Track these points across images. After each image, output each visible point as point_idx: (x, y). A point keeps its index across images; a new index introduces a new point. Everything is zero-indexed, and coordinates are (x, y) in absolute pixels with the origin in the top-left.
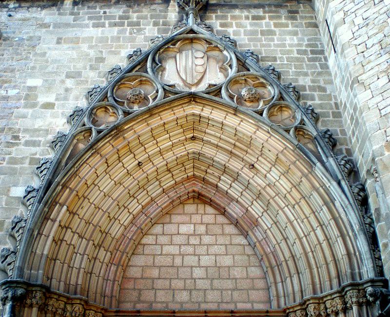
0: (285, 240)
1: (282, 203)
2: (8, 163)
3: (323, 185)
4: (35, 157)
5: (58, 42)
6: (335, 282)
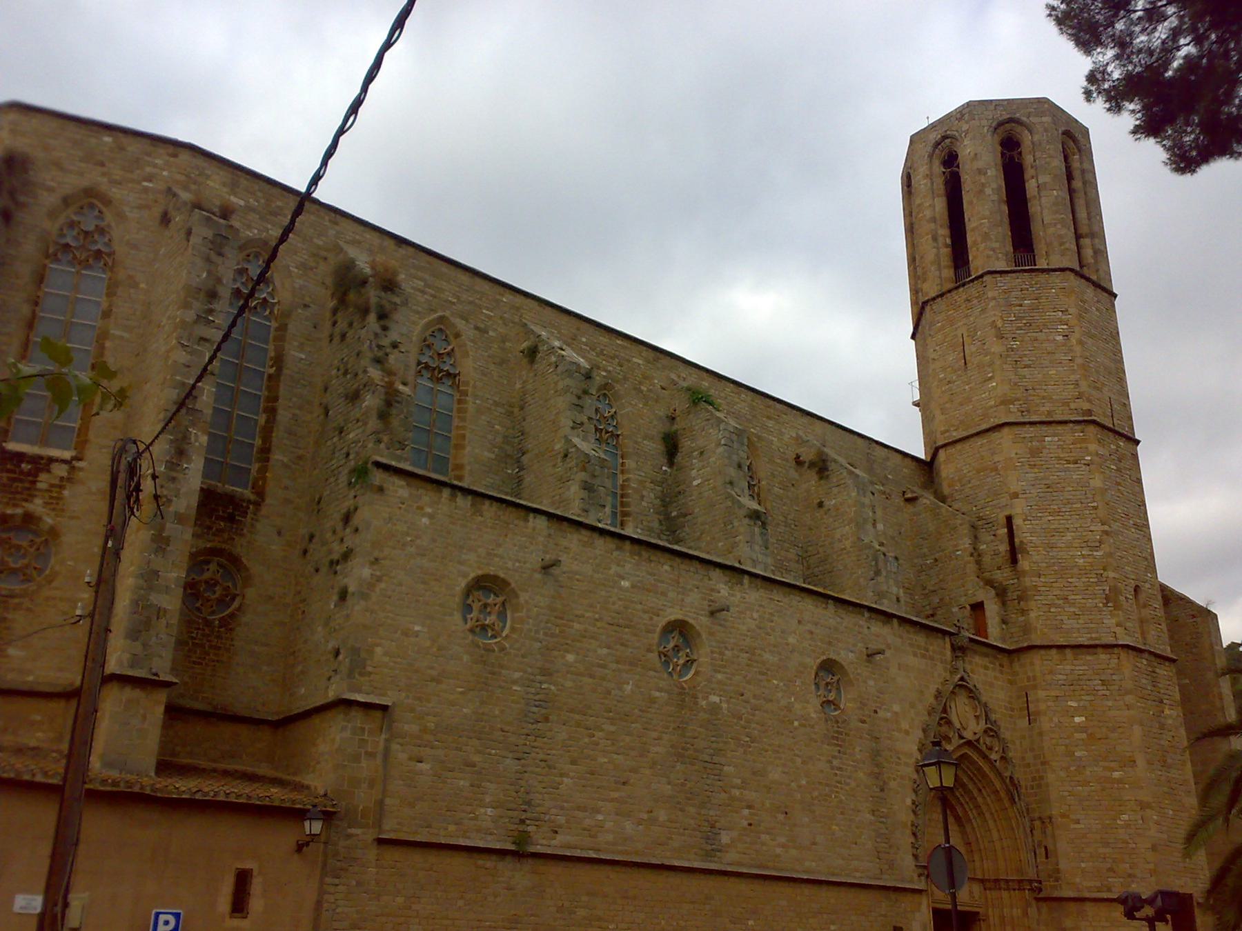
5: (899, 669)
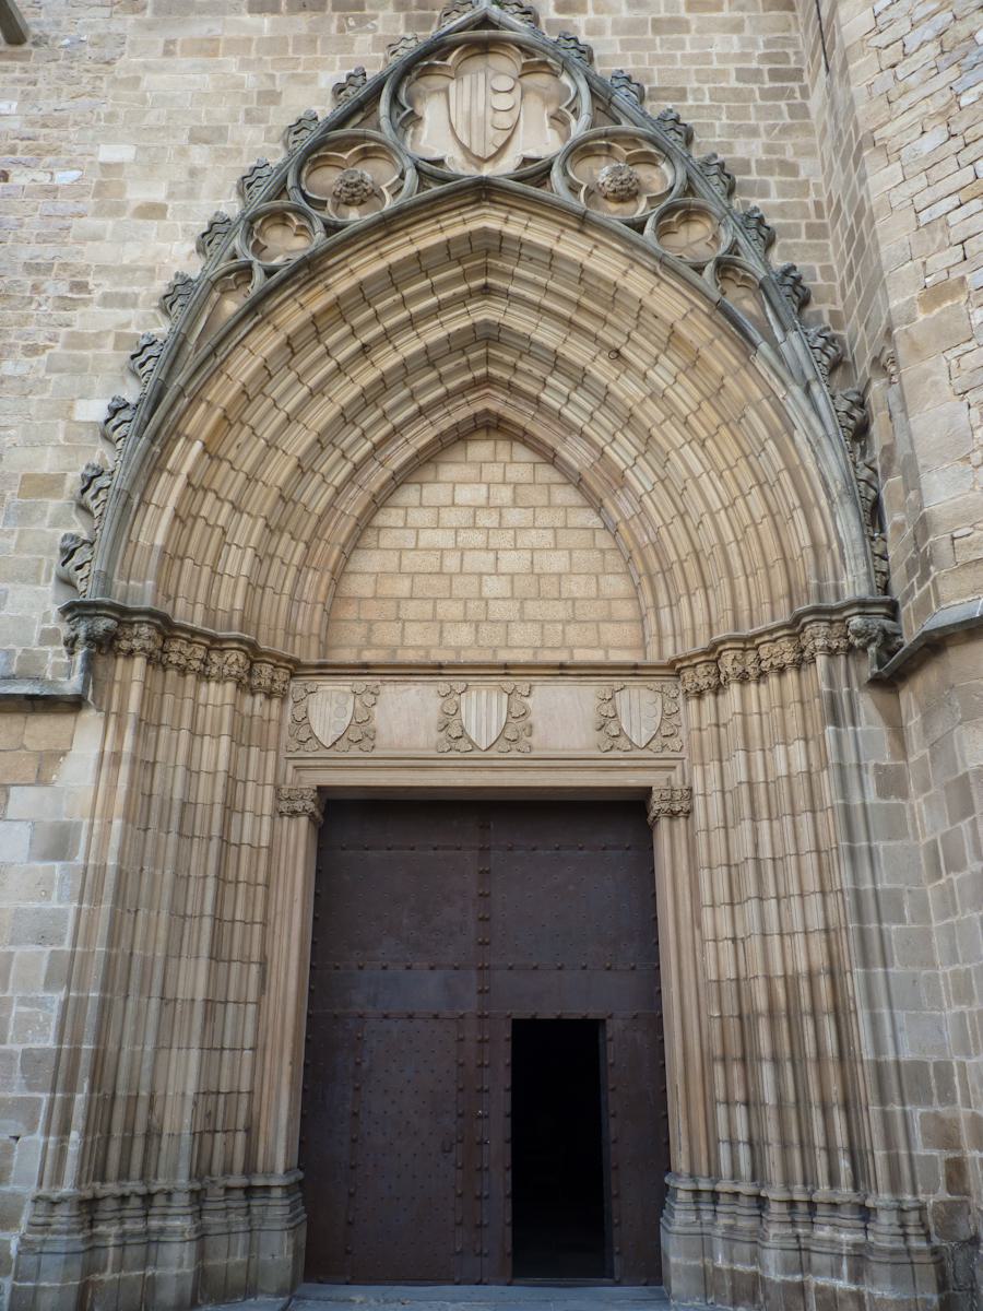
0: (682, 516)
1: (679, 437)
2: (66, 346)
3: (771, 394)
4: (127, 331)
5: (168, 52)
6: (783, 604)
